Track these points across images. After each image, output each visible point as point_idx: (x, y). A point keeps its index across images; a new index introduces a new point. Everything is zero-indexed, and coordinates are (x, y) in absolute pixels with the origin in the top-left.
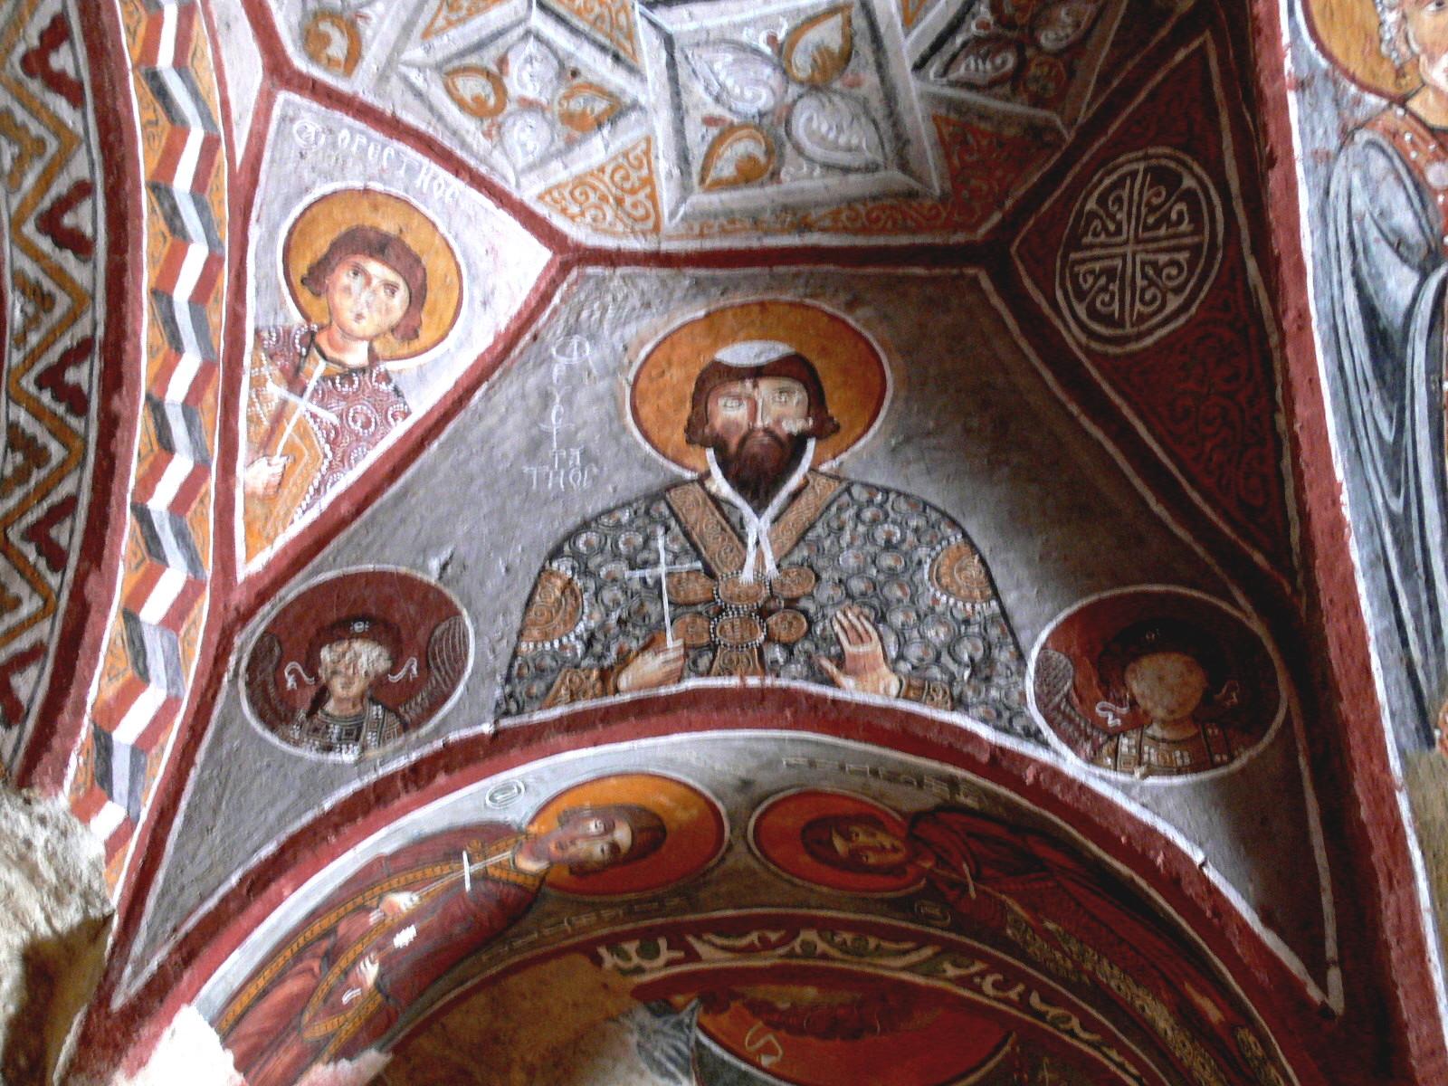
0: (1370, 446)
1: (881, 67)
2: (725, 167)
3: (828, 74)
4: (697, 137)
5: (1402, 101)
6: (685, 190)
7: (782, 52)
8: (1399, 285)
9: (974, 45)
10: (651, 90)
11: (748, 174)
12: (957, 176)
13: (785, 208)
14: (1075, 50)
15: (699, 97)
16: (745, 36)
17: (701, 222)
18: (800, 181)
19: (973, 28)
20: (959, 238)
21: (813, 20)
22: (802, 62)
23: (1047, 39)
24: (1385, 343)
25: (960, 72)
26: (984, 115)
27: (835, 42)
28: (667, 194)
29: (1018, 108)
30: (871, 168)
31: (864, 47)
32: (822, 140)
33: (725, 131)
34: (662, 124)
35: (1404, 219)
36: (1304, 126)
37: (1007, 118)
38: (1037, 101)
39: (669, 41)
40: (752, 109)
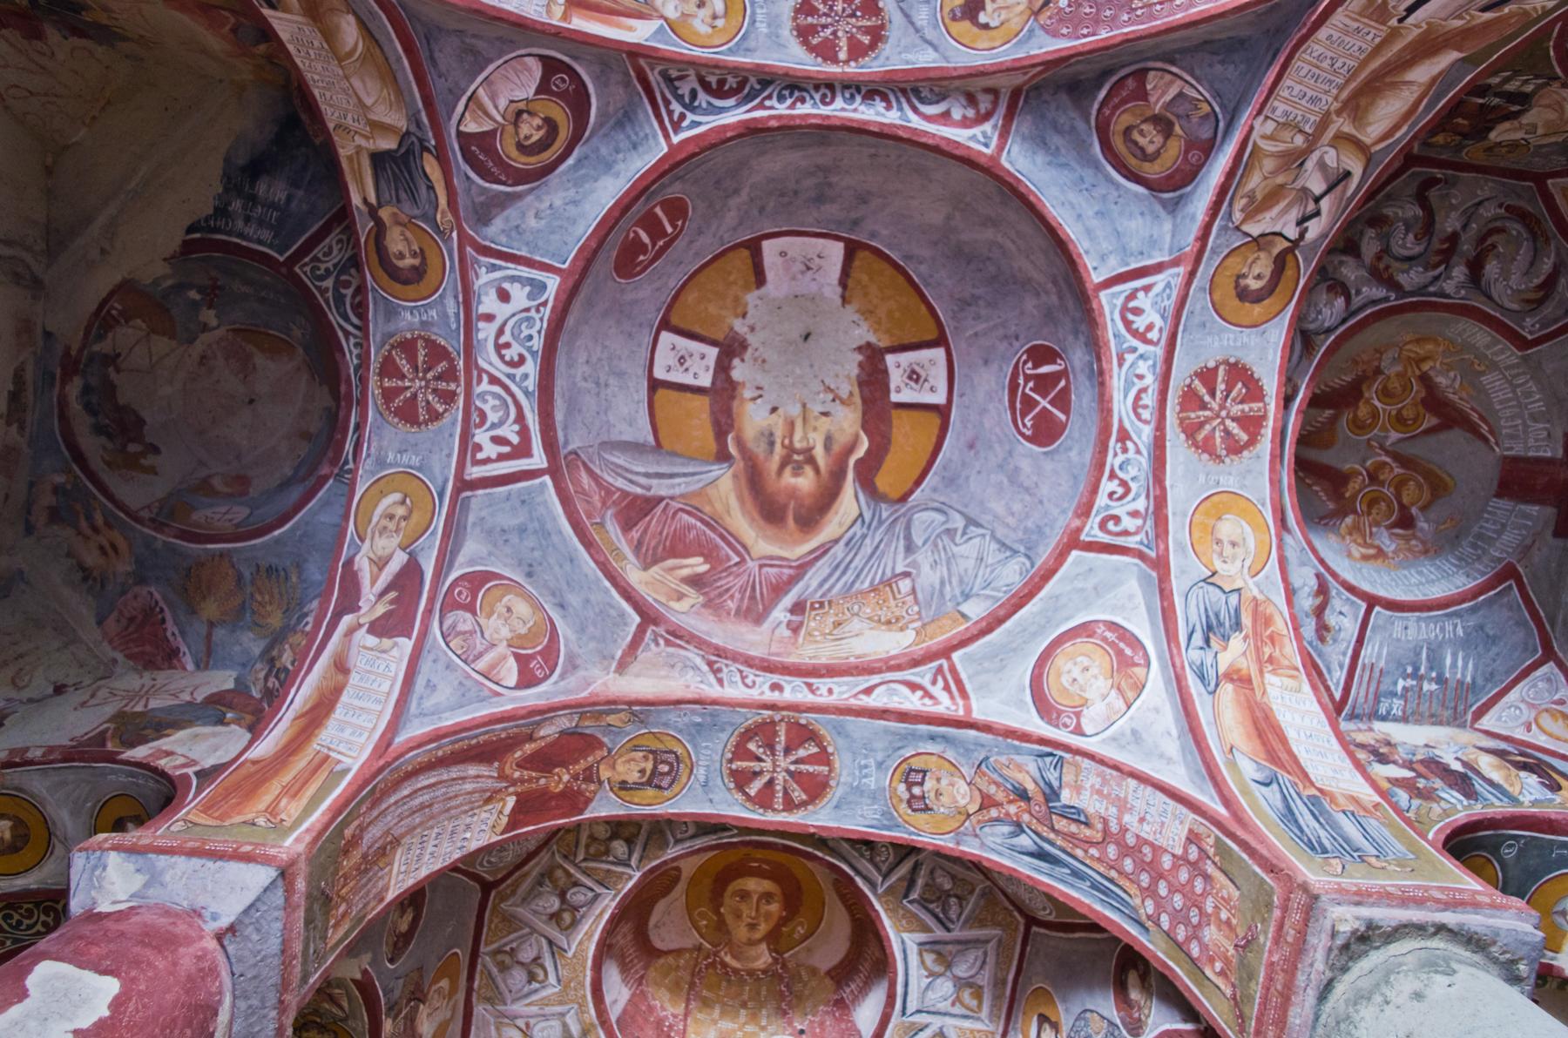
0: (1071, 879)
1: (946, 943)
2: (974, 1003)
3: (946, 961)
4: (958, 1010)
5: (969, 816)
6: (978, 1019)
7: (931, 974)
8: (1025, 841)
9: (945, 911)
10: (936, 1022)
11: (978, 994)
12: (996, 924)
13: (995, 985)
14: (953, 877)
15: (942, 1006)
16: (923, 985)
17: (993, 1016)
18: (984, 979)
19: (938, 910)
20: (1022, 928)
21: (923, 962)
22: (938, 969)
23: (947, 886)
24: (1041, 855)
25: (954, 917)
26: (973, 911)
27: (933, 956)
28: (979, 1026)
29: (973, 900)
30: (985, 954)
31: (937, 947)
32: (970, 968)
33: (958, 1000)
34: (949, 1021)
35: (1006, 829)
36: (971, 848)
37: (976, 904)
38: (972, 892)
39: (919, 1011)
40: (952, 989)
